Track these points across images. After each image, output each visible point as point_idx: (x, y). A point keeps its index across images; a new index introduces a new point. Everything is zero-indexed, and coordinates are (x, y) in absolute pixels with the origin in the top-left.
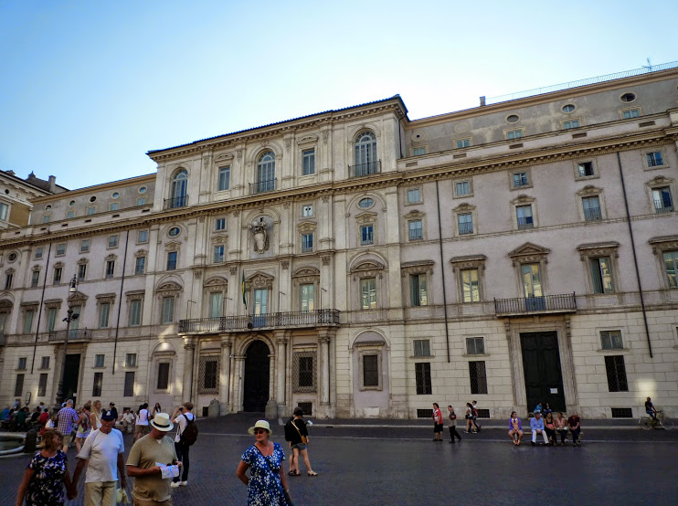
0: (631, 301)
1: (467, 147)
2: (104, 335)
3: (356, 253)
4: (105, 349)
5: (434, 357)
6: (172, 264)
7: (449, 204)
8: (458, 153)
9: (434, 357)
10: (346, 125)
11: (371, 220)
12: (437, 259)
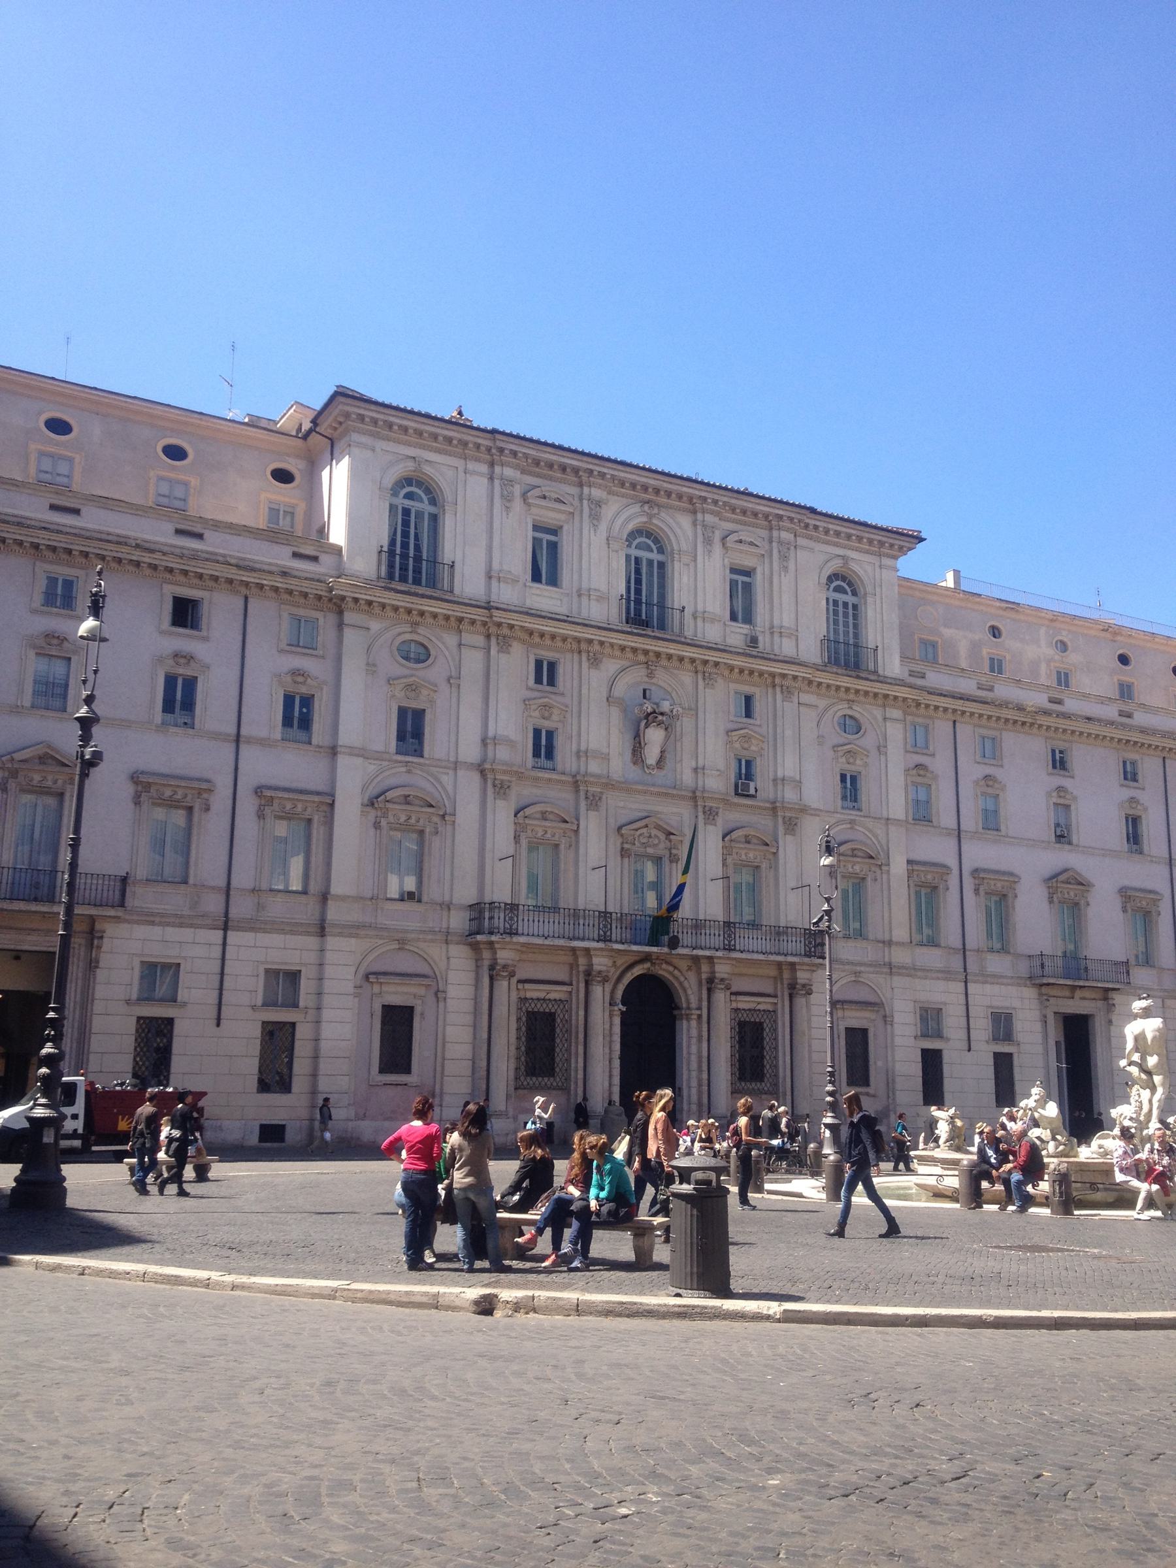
2: (174, 900)
3: (833, 821)
4: (194, 949)
5: (948, 1040)
6: (411, 730)
7: (971, 771)
11: (858, 762)
12: (952, 862)
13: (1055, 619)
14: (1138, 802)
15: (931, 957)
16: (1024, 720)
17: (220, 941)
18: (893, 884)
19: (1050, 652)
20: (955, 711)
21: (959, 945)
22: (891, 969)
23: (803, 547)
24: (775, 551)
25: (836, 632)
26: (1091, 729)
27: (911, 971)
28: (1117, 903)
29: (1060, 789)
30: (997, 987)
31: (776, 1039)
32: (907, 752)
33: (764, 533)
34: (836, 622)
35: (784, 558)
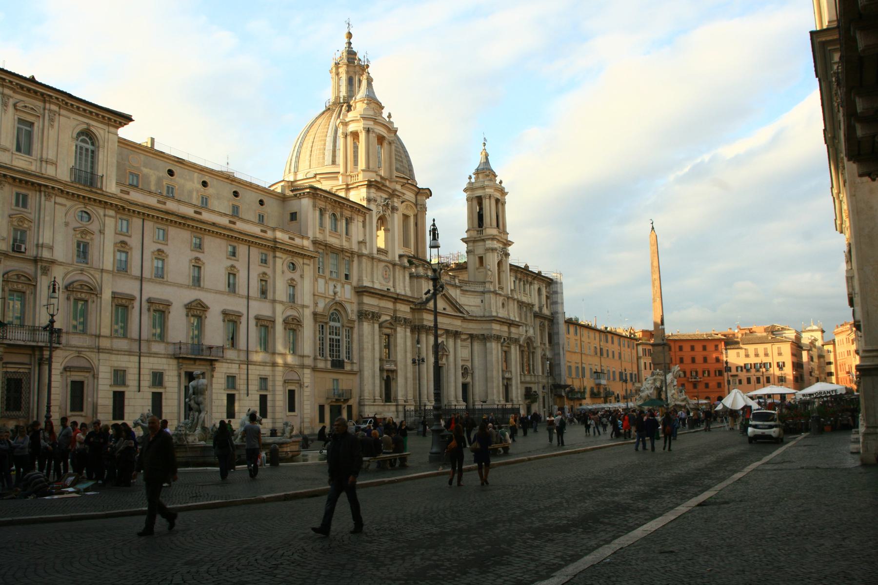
0: (243, 357)
1: (135, 187)
3: (71, 269)
5: (128, 386)
8: (161, 199)
9: (128, 386)
10: (73, 116)
12: (137, 294)
13: (202, 170)
14: (235, 267)
15: (122, 344)
16: (182, 222)
18: (103, 305)
19: (200, 186)
20: (144, 214)
21: (137, 337)
22: (99, 350)
23: (63, 116)
24: (47, 115)
25: (80, 164)
26: (214, 230)
27: (110, 351)
28: (221, 317)
29: (197, 259)
30: (156, 359)
31: (29, 388)
32: (116, 233)
33: (41, 104)
34: (80, 159)
35: (52, 120)
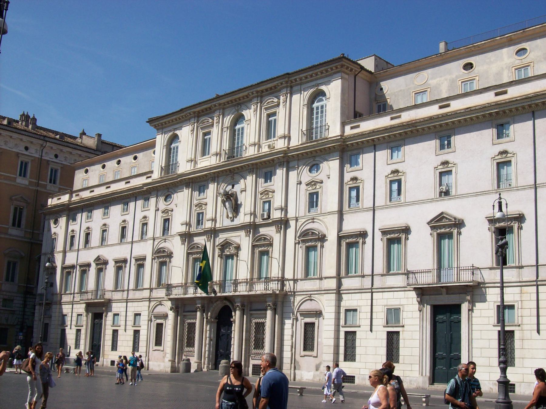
17: (535, 291)
